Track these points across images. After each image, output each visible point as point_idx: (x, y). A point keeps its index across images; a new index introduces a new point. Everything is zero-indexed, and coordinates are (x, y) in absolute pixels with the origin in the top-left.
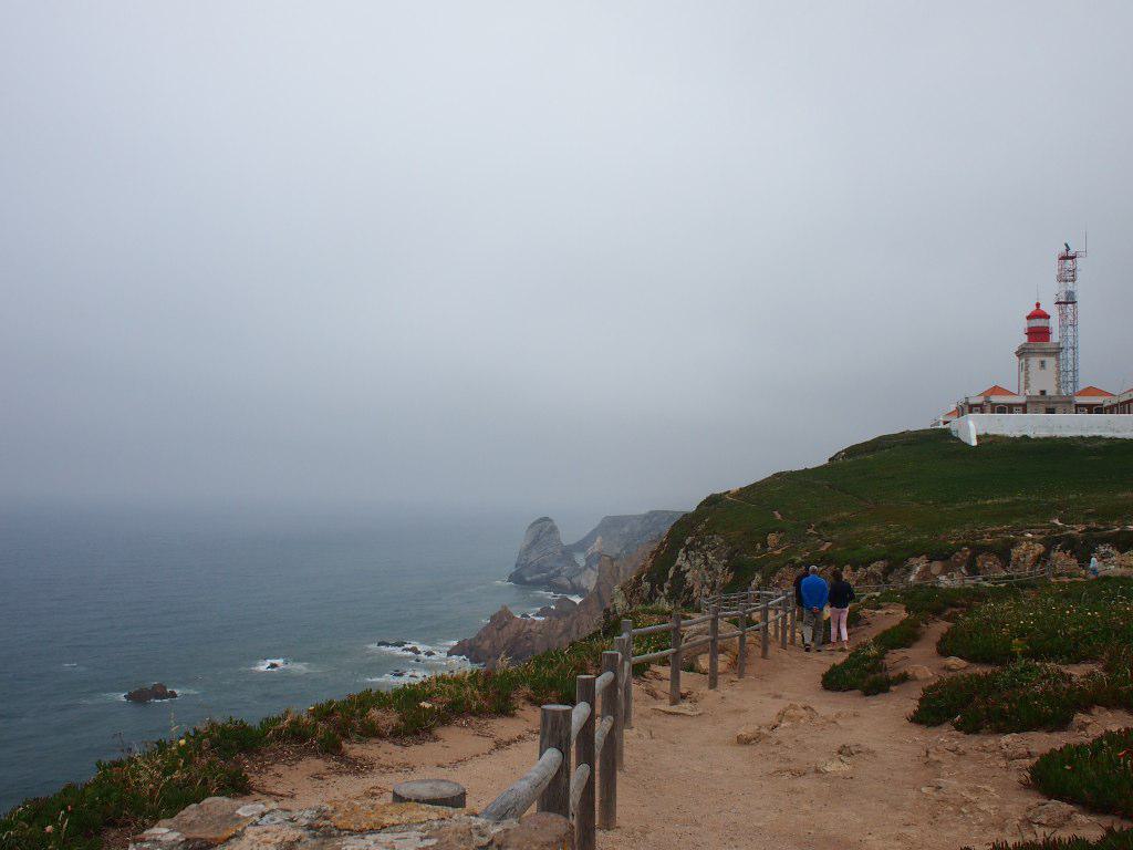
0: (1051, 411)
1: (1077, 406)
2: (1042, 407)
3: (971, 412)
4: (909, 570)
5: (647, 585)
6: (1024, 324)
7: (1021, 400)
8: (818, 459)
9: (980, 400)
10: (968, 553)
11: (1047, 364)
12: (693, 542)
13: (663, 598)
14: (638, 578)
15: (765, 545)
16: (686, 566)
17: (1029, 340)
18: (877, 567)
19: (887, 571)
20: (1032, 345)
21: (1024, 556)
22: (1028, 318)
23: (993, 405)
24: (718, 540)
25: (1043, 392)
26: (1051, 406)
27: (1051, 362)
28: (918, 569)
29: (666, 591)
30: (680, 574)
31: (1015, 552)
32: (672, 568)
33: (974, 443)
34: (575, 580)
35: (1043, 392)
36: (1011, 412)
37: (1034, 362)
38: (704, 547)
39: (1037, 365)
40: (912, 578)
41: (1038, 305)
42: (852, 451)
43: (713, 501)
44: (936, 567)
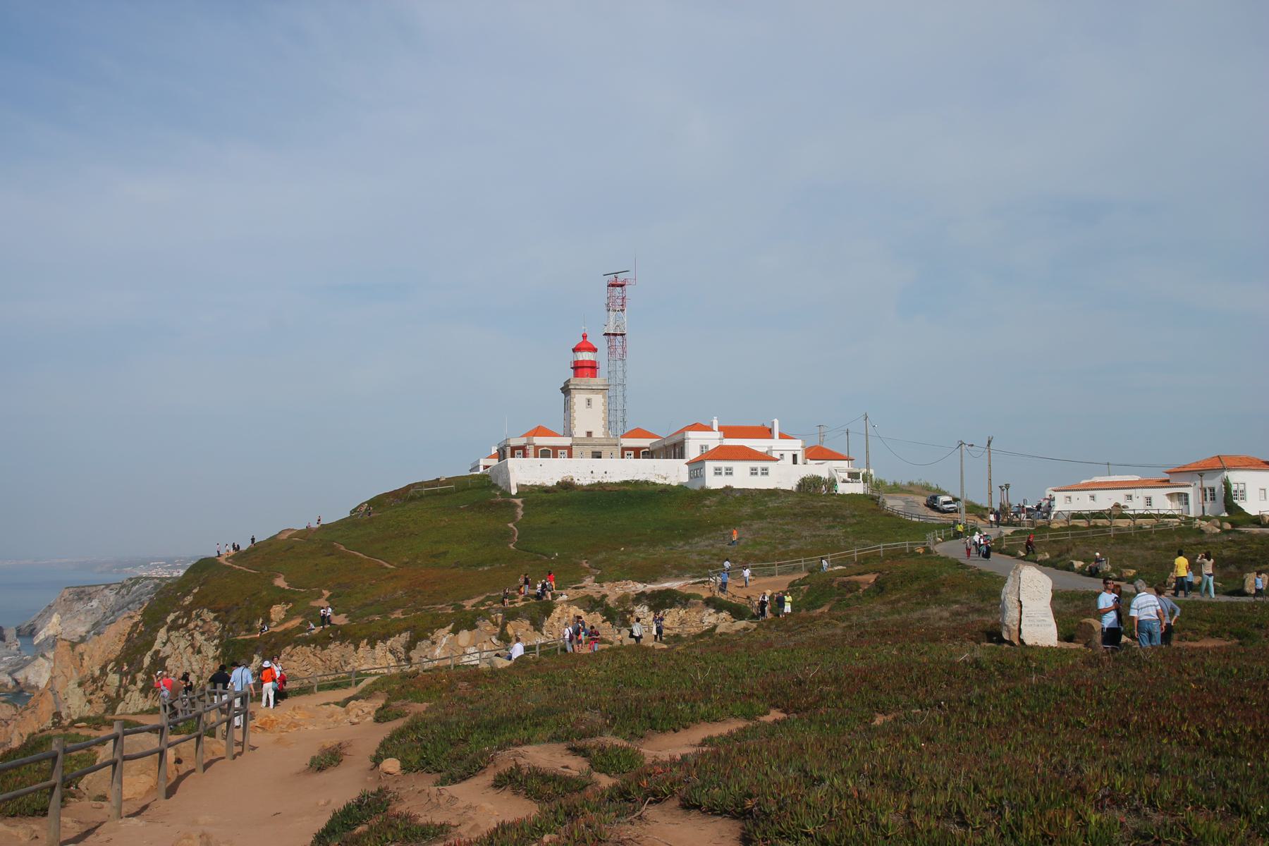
0: (597, 455)
1: (624, 449)
2: (589, 450)
3: (513, 456)
4: (434, 643)
5: (114, 679)
6: (572, 357)
7: (567, 441)
8: (337, 511)
9: (521, 442)
11: (593, 403)
12: (177, 618)
13: (136, 695)
14: (103, 669)
15: (268, 620)
16: (168, 650)
17: (576, 375)
19: (410, 646)
20: (578, 380)
22: (574, 350)
23: (537, 448)
24: (209, 616)
26: (597, 449)
27: (598, 400)
28: (444, 640)
29: (140, 684)
30: (159, 662)
32: (150, 653)
33: (514, 492)
34: (20, 676)
35: (589, 434)
36: (555, 456)
38: (191, 625)
39: (585, 403)
41: (585, 337)
42: (377, 503)
43: (204, 569)
44: (464, 636)
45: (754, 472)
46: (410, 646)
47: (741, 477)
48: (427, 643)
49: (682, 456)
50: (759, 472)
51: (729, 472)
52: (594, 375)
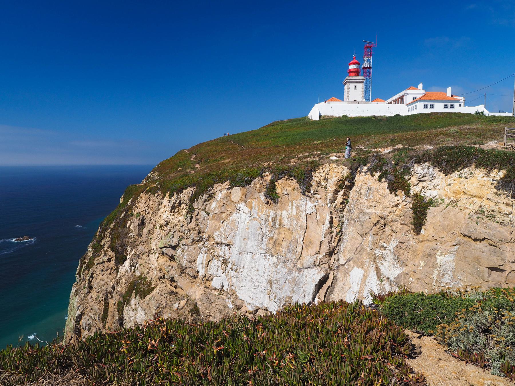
4: (211, 196)
10: (269, 178)
11: (357, 87)
18: (187, 194)
19: (193, 199)
20: (351, 77)
21: (326, 179)
25: (355, 101)
27: (360, 86)
31: (317, 176)
33: (318, 119)
37: (352, 85)
40: (213, 205)
44: (237, 193)
45: (446, 106)
46: (193, 199)
47: (439, 108)
48: (205, 196)
49: (402, 102)
50: (449, 106)
51: (432, 106)
52: (358, 75)
